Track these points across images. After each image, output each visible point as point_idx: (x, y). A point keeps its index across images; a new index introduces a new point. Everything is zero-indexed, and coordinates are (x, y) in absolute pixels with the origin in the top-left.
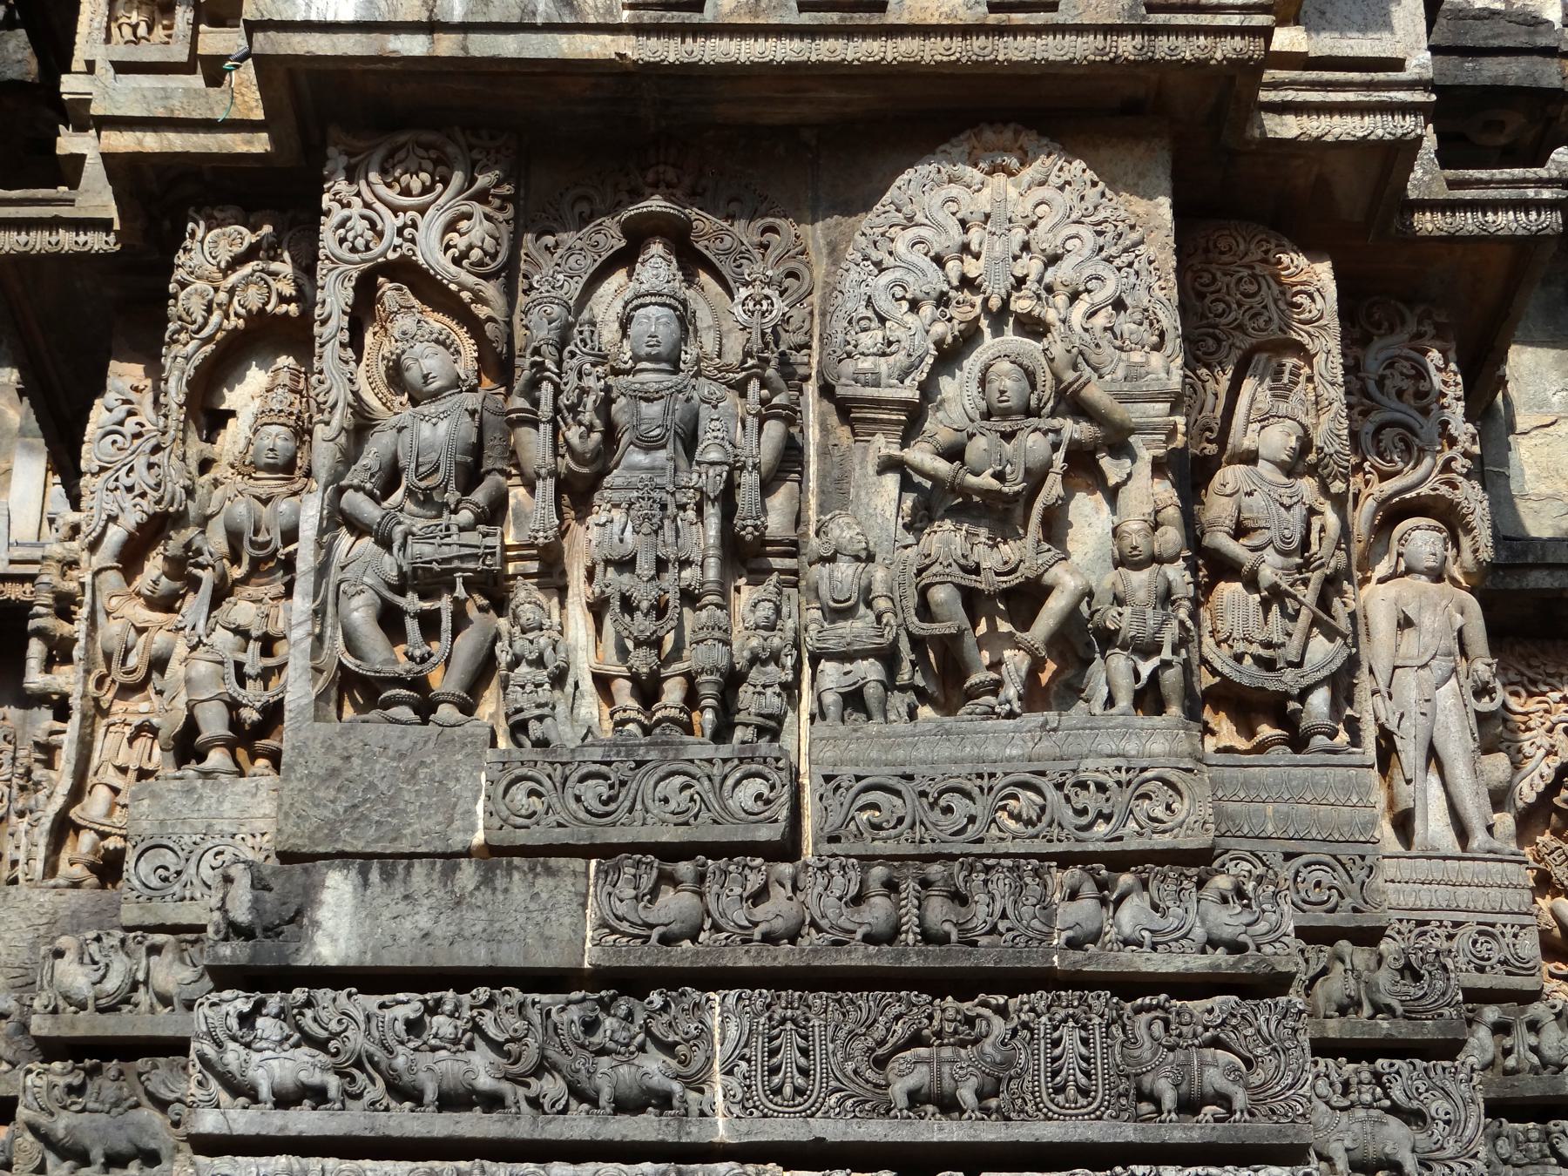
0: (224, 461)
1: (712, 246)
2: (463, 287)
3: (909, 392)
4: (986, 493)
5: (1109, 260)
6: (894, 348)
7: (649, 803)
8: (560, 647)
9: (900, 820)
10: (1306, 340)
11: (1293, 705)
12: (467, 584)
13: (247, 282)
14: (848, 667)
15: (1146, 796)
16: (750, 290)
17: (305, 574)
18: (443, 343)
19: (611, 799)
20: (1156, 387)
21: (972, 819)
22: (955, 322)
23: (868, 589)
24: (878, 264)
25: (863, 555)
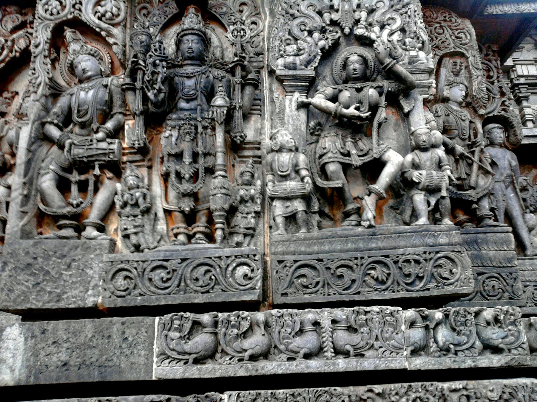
0: (11, 114)
1: (217, 10)
2: (102, 30)
3: (310, 72)
4: (351, 118)
5: (397, 10)
6: (302, 52)
7: (188, 282)
8: (148, 197)
9: (318, 283)
10: (465, 52)
11: (475, 206)
12: (101, 168)
13: (19, 38)
14: (288, 204)
15: (440, 266)
16: (235, 26)
17: (20, 165)
18: (93, 55)
19: (168, 279)
20: (422, 67)
21: (354, 281)
22: (329, 40)
23: (297, 165)
24: (292, 15)
25: (294, 149)
